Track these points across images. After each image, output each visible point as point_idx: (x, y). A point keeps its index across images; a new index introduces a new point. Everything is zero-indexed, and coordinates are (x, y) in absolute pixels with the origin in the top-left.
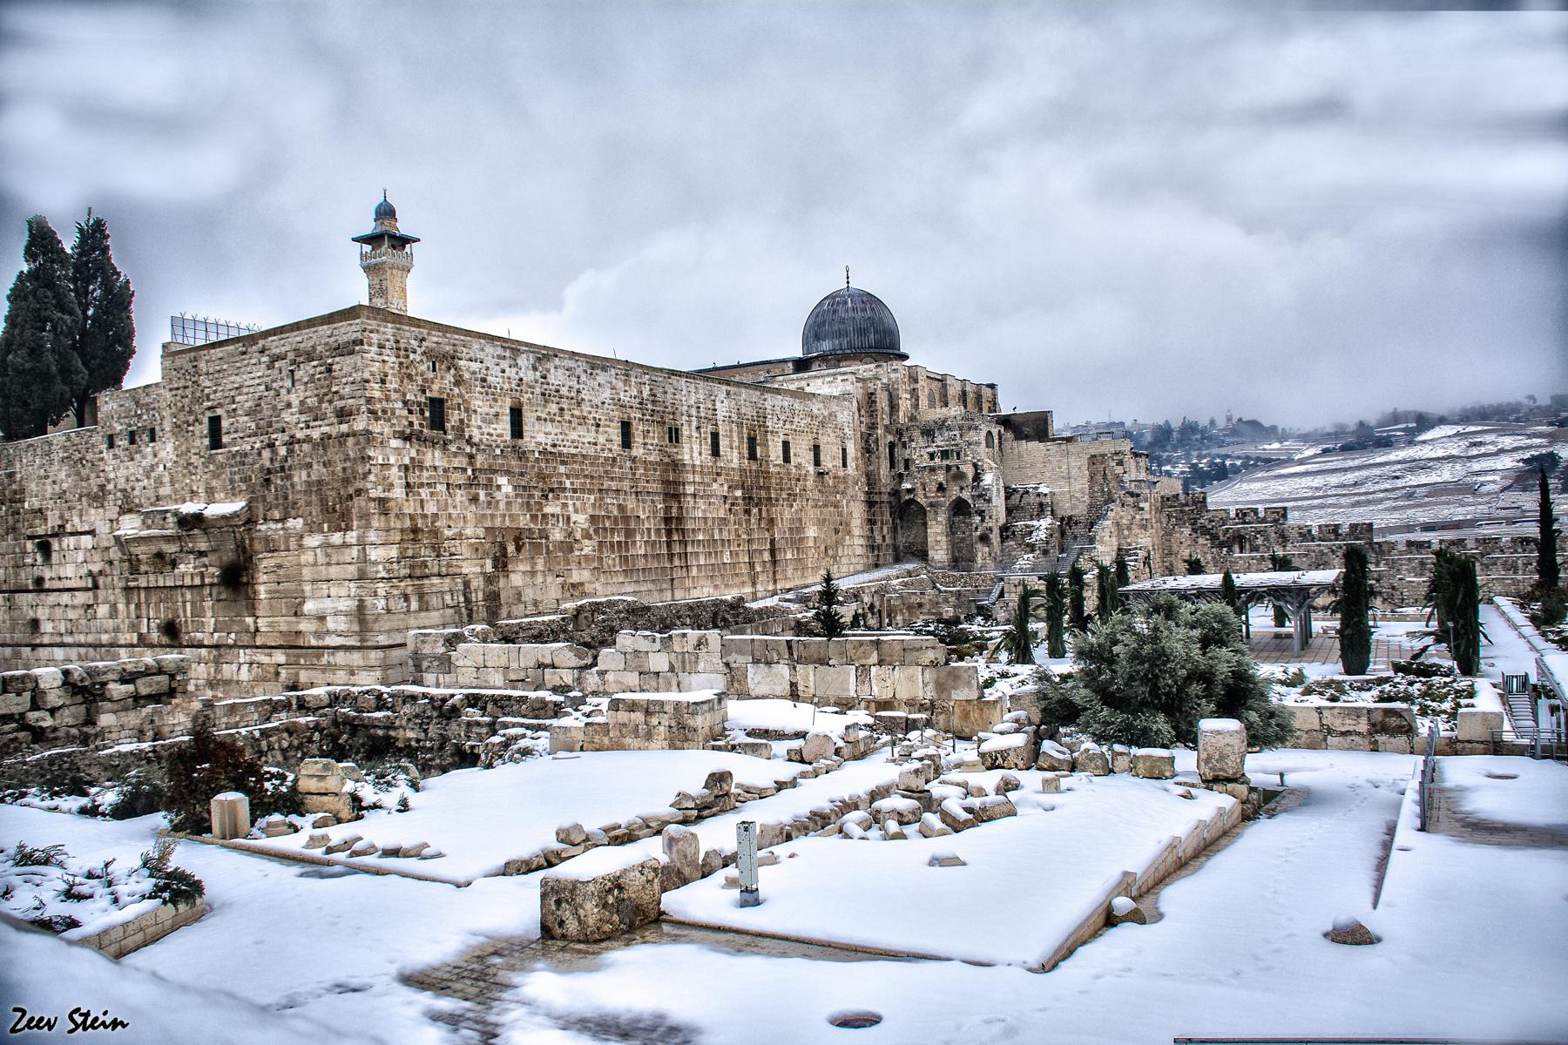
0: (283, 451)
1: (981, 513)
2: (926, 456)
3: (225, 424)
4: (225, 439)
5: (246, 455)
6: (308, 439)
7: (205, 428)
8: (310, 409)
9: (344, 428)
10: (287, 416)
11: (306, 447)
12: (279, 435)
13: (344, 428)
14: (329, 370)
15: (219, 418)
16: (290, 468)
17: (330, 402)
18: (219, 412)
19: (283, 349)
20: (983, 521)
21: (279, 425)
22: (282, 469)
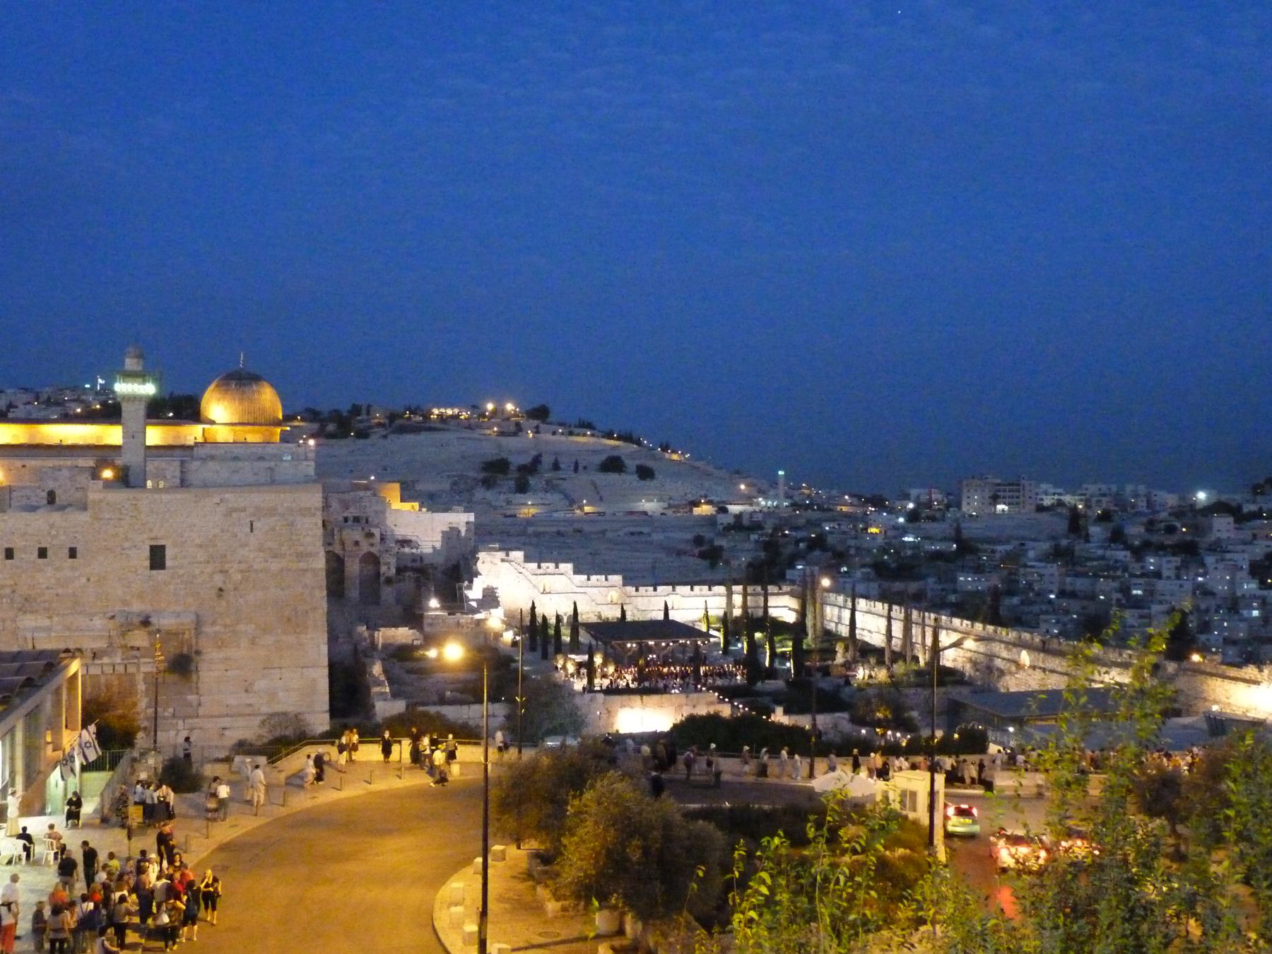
0: (239, 577)
3: (169, 553)
4: (168, 563)
6: (266, 571)
7: (147, 553)
9: (302, 565)
10: (244, 552)
13: (302, 565)
18: (161, 543)
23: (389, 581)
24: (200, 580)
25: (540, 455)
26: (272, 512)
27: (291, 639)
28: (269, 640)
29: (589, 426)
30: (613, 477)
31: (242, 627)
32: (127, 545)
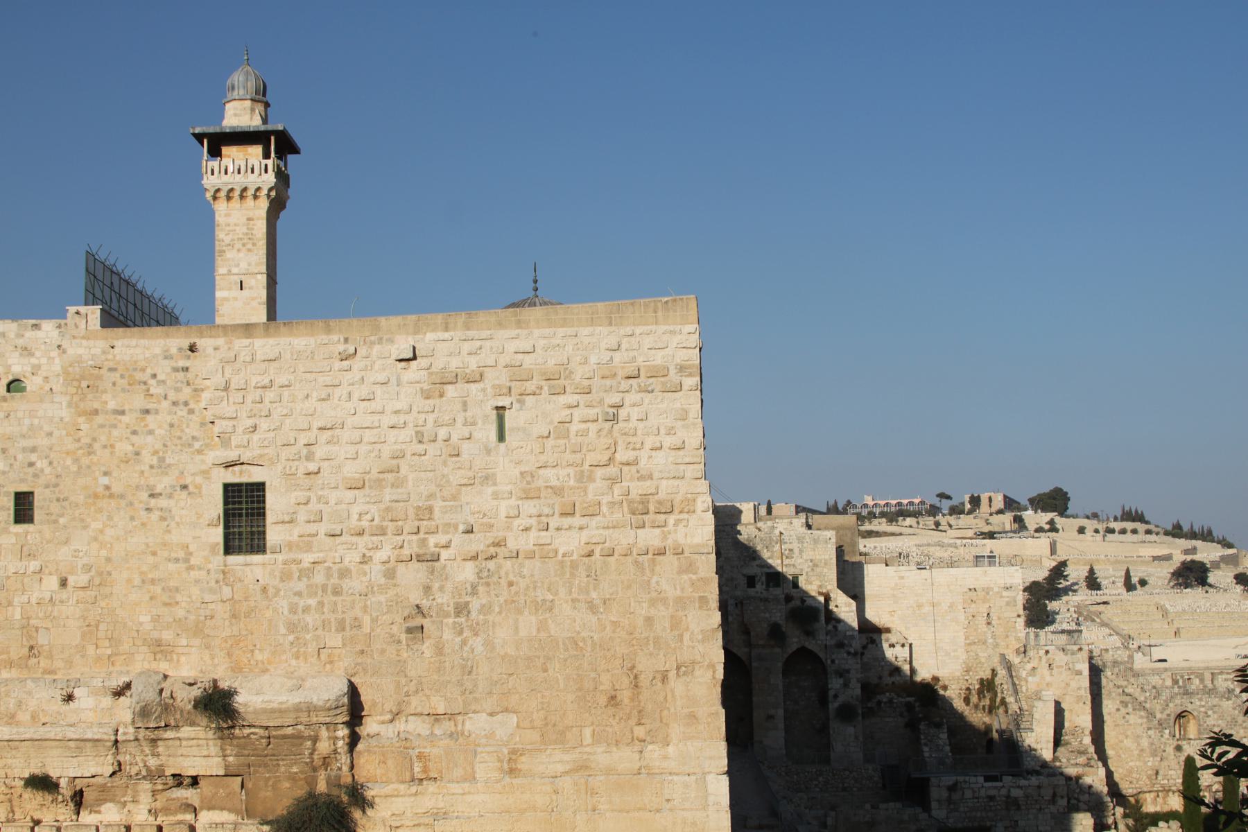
0: (468, 572)
1: (842, 674)
2: (743, 581)
3: (274, 503)
4: (273, 535)
5: (344, 573)
6: (544, 553)
7: (216, 507)
8: (558, 491)
9: (650, 537)
10: (478, 501)
11: (537, 563)
12: (457, 539)
13: (650, 537)
14: (615, 418)
15: (260, 487)
16: (485, 609)
17: (614, 481)
18: (254, 475)
19: (473, 363)
20: (846, 685)
21: (465, 517)
22: (461, 609)
23: (846, 713)
24: (355, 584)
25: (1063, 564)
26: (556, 381)
27: (625, 758)
28: (556, 760)
29: (1139, 518)
30: (1193, 596)
31: (476, 724)
32: (162, 484)
